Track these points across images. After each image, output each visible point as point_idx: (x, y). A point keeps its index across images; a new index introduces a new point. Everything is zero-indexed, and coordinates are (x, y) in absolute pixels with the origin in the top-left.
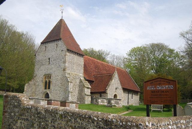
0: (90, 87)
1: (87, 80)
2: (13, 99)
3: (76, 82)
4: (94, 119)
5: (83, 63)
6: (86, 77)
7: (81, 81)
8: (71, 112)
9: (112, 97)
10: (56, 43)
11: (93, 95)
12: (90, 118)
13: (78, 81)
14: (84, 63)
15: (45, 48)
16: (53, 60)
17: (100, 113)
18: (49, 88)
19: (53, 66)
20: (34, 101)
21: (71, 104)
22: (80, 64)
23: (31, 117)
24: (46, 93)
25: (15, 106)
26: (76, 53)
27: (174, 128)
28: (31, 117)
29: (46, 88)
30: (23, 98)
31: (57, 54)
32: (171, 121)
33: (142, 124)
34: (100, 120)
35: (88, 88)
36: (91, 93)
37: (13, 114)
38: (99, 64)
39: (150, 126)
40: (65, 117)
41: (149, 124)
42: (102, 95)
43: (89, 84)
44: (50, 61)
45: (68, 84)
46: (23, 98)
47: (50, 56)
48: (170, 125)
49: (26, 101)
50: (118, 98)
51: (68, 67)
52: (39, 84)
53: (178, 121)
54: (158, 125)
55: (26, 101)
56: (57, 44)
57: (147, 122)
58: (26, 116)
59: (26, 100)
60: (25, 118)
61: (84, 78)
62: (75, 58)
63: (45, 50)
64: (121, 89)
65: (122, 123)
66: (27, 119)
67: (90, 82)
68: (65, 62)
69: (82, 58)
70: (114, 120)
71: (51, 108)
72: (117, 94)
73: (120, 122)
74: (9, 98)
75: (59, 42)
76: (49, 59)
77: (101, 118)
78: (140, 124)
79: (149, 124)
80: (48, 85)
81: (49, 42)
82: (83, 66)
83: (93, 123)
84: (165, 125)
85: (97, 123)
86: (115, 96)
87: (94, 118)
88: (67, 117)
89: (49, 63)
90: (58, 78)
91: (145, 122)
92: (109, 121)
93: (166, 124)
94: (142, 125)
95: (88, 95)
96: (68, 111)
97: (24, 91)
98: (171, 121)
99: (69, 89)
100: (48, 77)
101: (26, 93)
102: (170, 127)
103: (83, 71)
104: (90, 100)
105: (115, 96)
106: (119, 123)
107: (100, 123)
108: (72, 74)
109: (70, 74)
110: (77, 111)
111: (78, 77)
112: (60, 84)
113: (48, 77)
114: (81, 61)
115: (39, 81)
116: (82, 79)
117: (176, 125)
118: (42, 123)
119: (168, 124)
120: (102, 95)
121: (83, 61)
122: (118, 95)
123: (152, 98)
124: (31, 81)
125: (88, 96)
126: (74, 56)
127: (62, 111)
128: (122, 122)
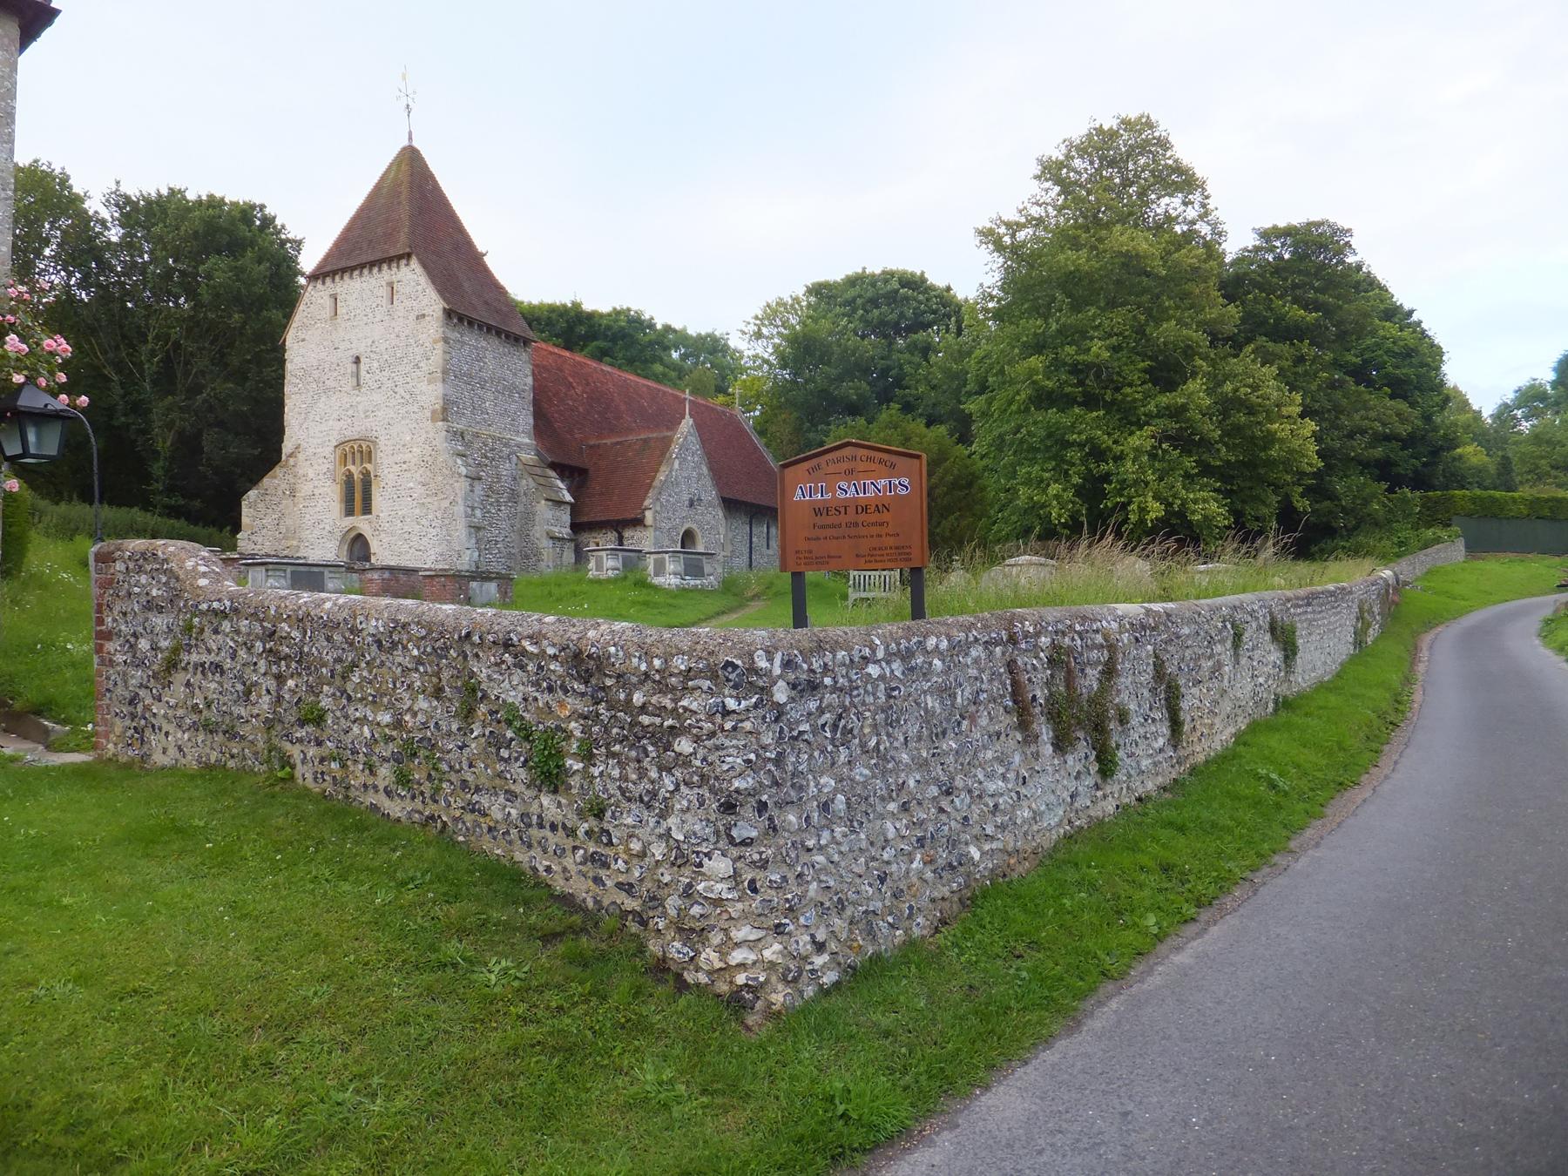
0: (568, 498)
2: (140, 570)
3: (499, 476)
4: (524, 652)
5: (530, 380)
8: (418, 623)
9: (675, 542)
10: (386, 274)
11: (585, 537)
12: (507, 645)
13: (506, 469)
14: (534, 380)
15: (328, 302)
16: (376, 365)
17: (550, 619)
18: (367, 509)
19: (377, 397)
20: (289, 575)
21: (474, 584)
22: (512, 388)
23: (234, 656)
24: (353, 534)
25: (151, 606)
26: (490, 328)
27: (892, 671)
28: (234, 656)
29: (350, 512)
30: (189, 564)
31: (393, 336)
32: (878, 642)
33: (739, 662)
34: (551, 651)
35: (559, 503)
36: (576, 527)
37: (144, 644)
39: (777, 671)
40: (394, 645)
41: (771, 660)
42: (627, 534)
43: (561, 485)
44: (363, 373)
46: (189, 564)
47: (360, 348)
48: (877, 662)
49: (204, 575)
50: (700, 549)
51: (454, 403)
52: (317, 492)
53: (915, 640)
54: (815, 666)
55: (204, 575)
56: (391, 285)
57: (760, 652)
58: (209, 651)
59: (203, 569)
60: (207, 659)
61: (538, 454)
62: (489, 355)
63: (328, 312)
64: (710, 504)
65: (650, 664)
66: (218, 668)
67: (563, 470)
69: (525, 356)
70: (612, 649)
71: (328, 605)
72: (694, 526)
73: (640, 658)
74: (120, 566)
75: (404, 269)
76: (357, 360)
77: (554, 645)
78: (728, 664)
79: (771, 660)
80: (358, 496)
81: (352, 269)
83: (522, 667)
84: (852, 661)
85: (540, 668)
86: (688, 538)
87: (526, 643)
88: (405, 647)
89: (358, 385)
90: (408, 457)
91: (751, 655)
92: (590, 656)
93: (856, 660)
94: (735, 667)
95: (559, 539)
96: (402, 618)
98: (878, 642)
100: (358, 456)
101: (253, 537)
102: (873, 670)
104: (573, 561)
105: (688, 538)
106: (635, 661)
107: (552, 667)
108: (477, 435)
109: (468, 437)
110: (448, 616)
111: (506, 451)
112: (422, 490)
113: (358, 456)
114: (518, 370)
115: (311, 475)
116: (529, 457)
117: (903, 659)
118: (291, 683)
119: (864, 658)
120: (627, 534)
121: (528, 369)
122: (698, 531)
123: (818, 539)
125: (558, 544)
126: (484, 344)
127: (377, 620)
128: (647, 655)
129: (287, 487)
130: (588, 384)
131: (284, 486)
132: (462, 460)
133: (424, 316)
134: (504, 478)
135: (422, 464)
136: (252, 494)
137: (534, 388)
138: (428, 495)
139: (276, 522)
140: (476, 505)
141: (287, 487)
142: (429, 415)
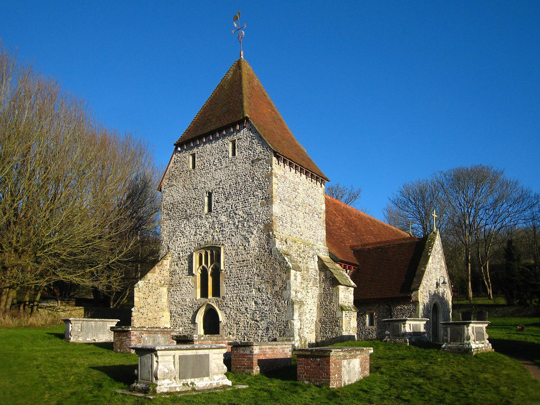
1: (341, 262)
5: (324, 207)
6: (333, 251)
7: (322, 267)
13: (314, 265)
22: (314, 211)
38: (353, 217)
45: (289, 278)
68: (268, 200)
82: (323, 216)
97: (133, 306)
99: (293, 293)
101: (141, 310)
103: (324, 233)
111: (312, 252)
116: (325, 256)
121: (321, 198)
124: (155, 272)
129: (163, 279)
130: (343, 215)
131: (160, 278)
132: (288, 257)
133: (259, 160)
134: (310, 270)
135: (257, 261)
136: (141, 283)
137: (327, 212)
138: (261, 283)
139: (156, 300)
140: (298, 289)
141: (163, 279)
142: (262, 227)
